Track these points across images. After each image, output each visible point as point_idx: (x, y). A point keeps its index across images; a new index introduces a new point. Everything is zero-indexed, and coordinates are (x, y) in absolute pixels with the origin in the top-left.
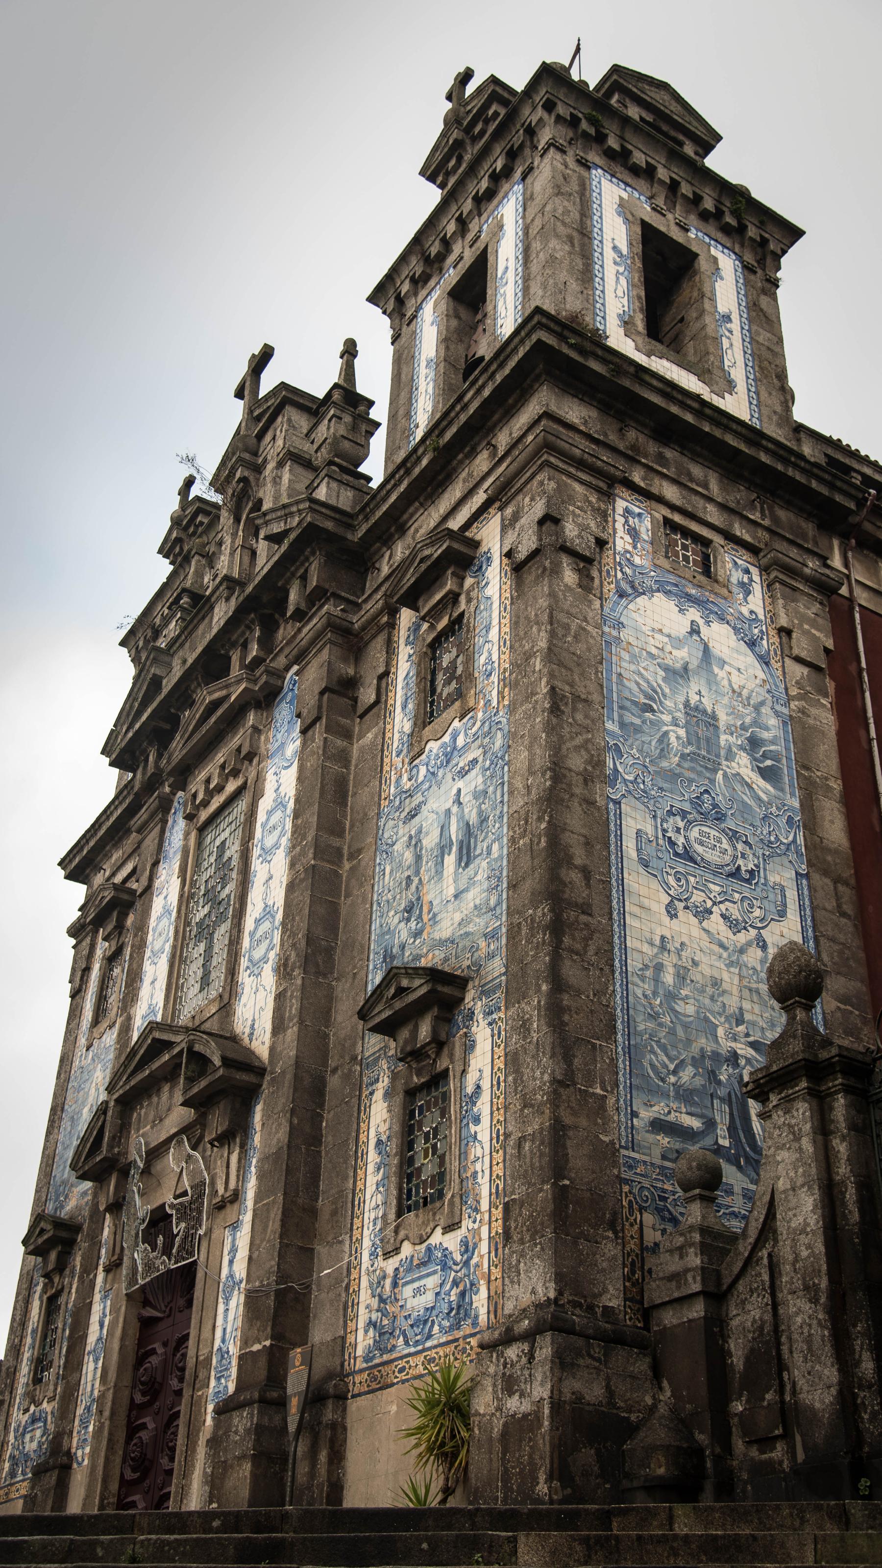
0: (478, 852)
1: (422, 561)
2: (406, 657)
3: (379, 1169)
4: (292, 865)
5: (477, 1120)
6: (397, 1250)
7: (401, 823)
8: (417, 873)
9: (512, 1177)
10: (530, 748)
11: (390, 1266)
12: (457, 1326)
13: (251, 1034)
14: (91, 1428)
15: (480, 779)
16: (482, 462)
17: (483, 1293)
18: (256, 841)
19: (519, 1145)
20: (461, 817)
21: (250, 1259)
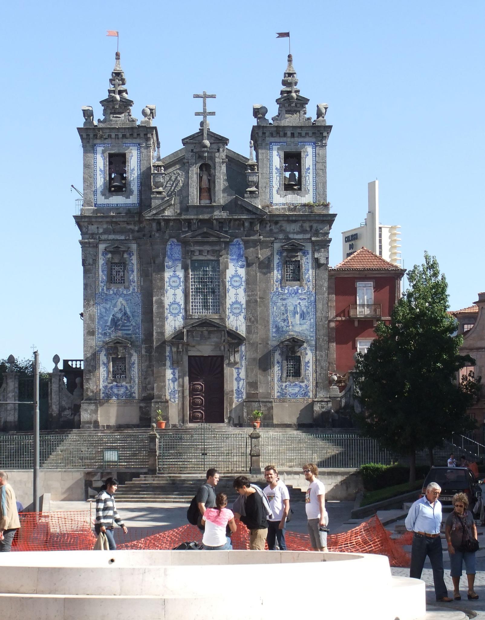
0: (307, 318)
1: (293, 245)
2: (277, 258)
3: (279, 367)
4: (248, 296)
5: (309, 367)
6: (286, 382)
7: (279, 300)
8: (287, 313)
9: (319, 377)
10: (323, 305)
11: (284, 384)
12: (305, 397)
13: (237, 330)
14: (177, 395)
15: (307, 304)
16: (307, 226)
17: (311, 393)
18: (227, 280)
19: (320, 374)
20: (301, 309)
21: (247, 376)
